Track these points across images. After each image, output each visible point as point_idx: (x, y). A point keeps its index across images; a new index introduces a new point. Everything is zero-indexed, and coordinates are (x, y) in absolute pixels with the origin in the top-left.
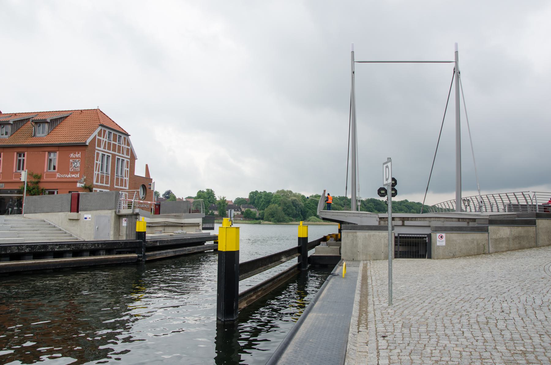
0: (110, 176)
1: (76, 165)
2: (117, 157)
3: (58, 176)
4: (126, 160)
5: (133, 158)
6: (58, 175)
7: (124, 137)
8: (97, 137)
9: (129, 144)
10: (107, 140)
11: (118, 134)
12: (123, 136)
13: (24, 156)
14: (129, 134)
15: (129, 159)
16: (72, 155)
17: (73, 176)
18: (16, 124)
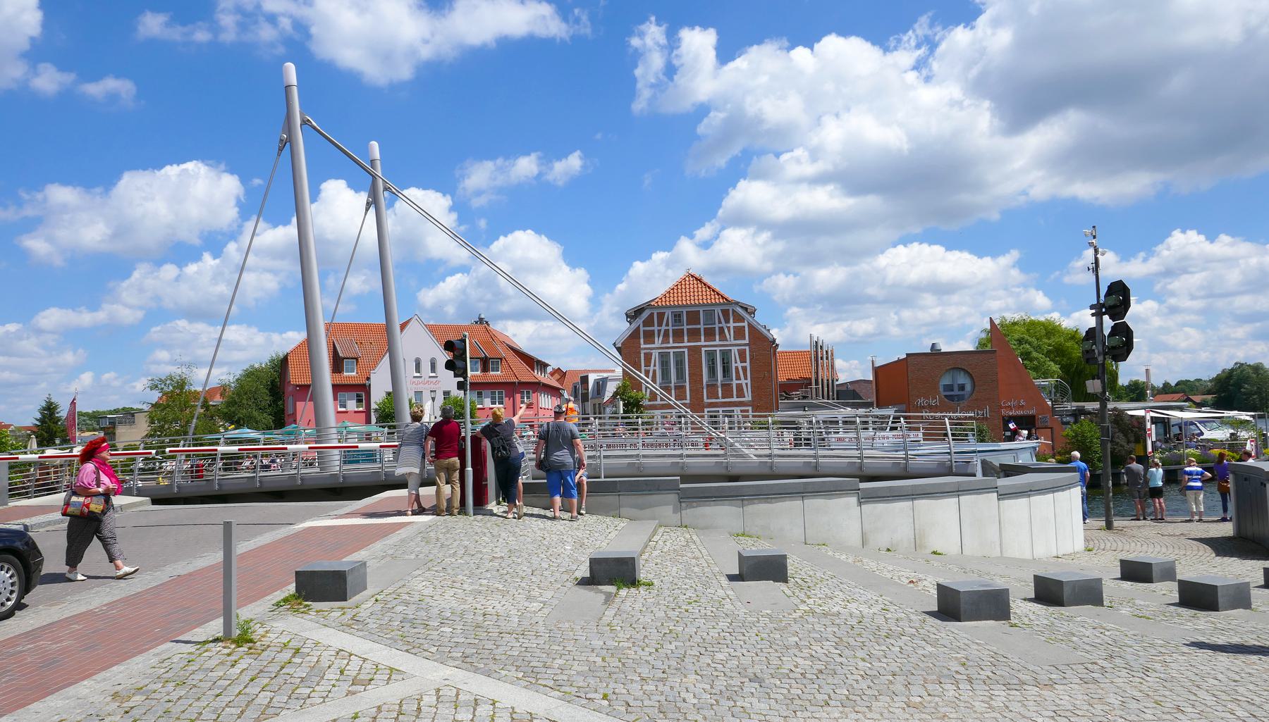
2: (703, 349)
8: (642, 329)
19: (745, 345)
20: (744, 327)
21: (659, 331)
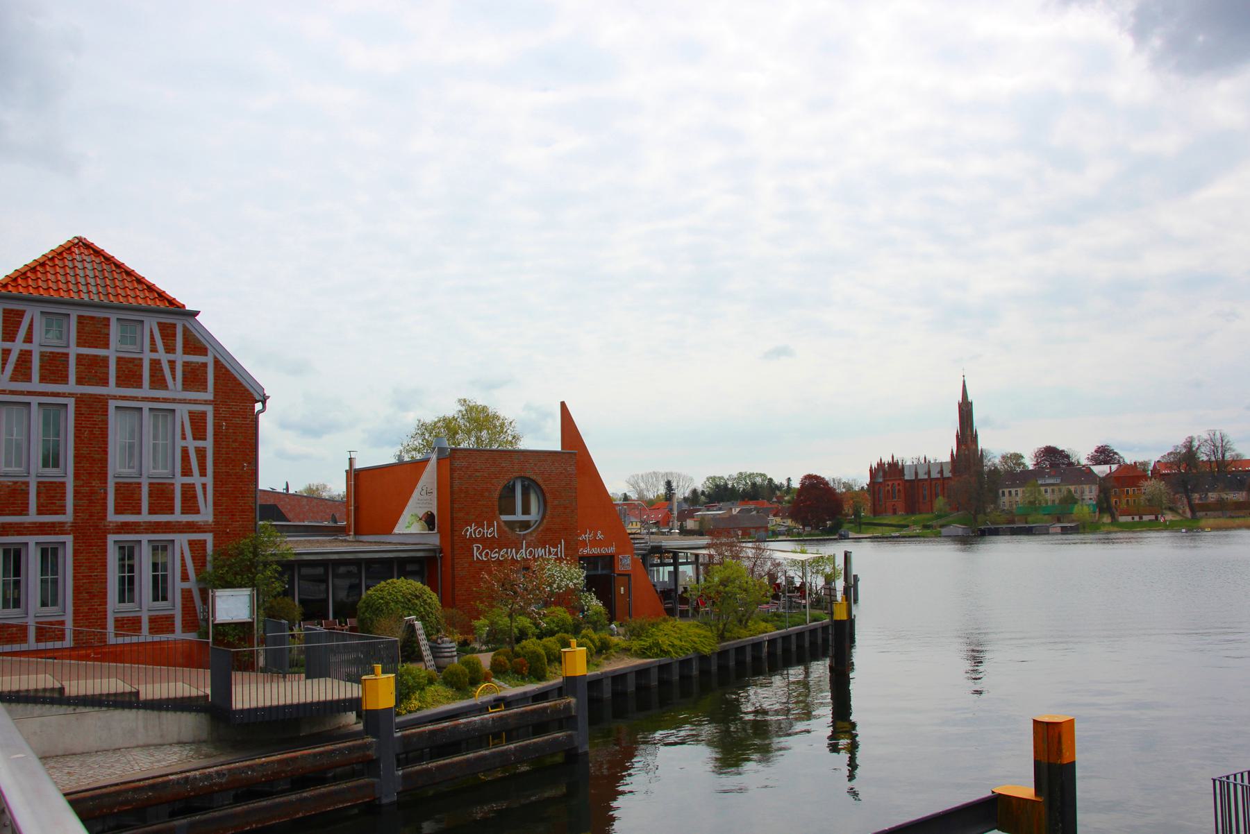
2: (112, 404)
7: (159, 324)
9: (197, 343)
15: (206, 402)
19: (206, 402)
20: (205, 365)
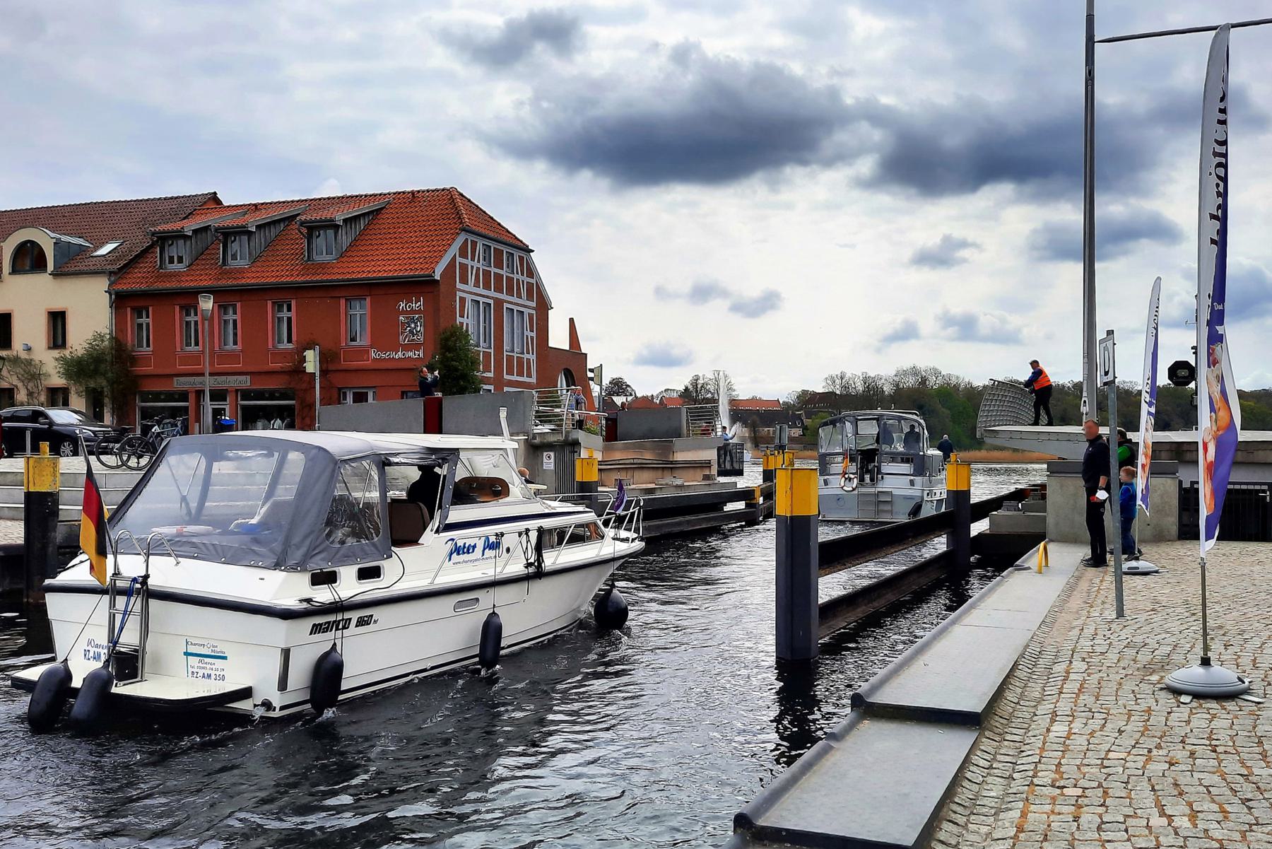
0: (492, 351)
1: (415, 328)
2: (506, 305)
3: (373, 355)
4: (526, 311)
5: (543, 306)
6: (373, 354)
8: (459, 259)
9: (531, 272)
10: (480, 265)
11: (505, 249)
12: (517, 254)
13: (289, 310)
14: (530, 248)
15: (533, 308)
16: (402, 305)
17: (410, 354)
18: (262, 231)
19: (533, 308)
21: (472, 267)
